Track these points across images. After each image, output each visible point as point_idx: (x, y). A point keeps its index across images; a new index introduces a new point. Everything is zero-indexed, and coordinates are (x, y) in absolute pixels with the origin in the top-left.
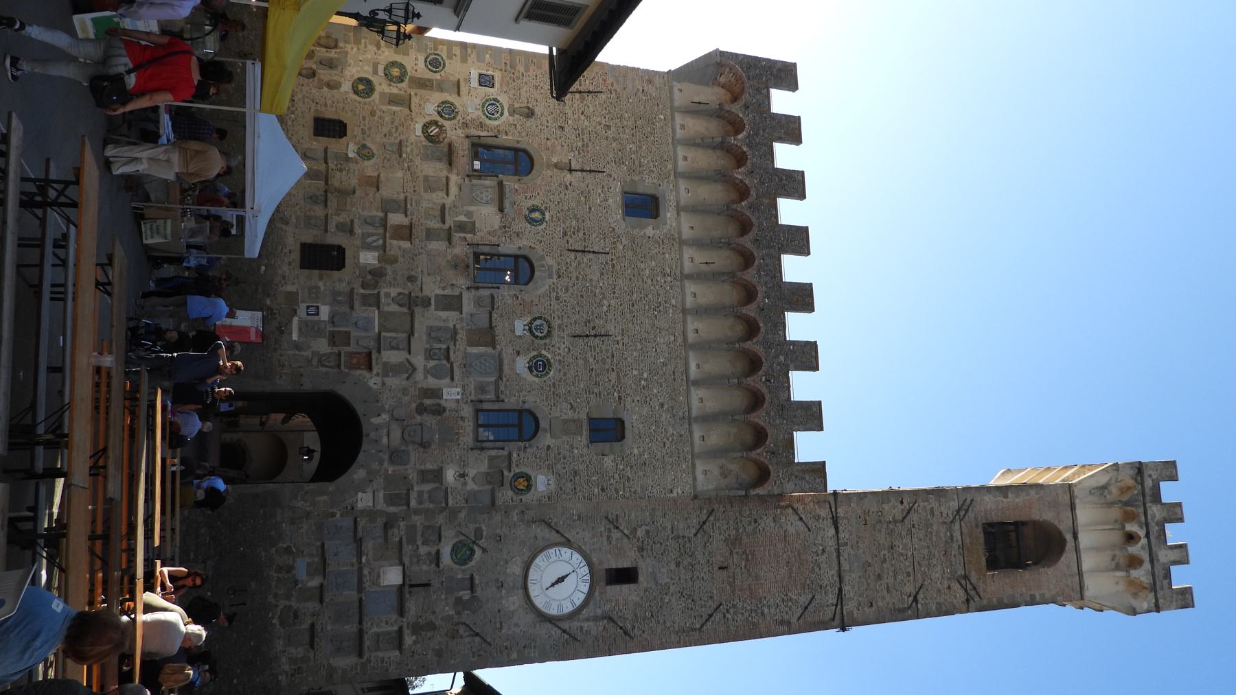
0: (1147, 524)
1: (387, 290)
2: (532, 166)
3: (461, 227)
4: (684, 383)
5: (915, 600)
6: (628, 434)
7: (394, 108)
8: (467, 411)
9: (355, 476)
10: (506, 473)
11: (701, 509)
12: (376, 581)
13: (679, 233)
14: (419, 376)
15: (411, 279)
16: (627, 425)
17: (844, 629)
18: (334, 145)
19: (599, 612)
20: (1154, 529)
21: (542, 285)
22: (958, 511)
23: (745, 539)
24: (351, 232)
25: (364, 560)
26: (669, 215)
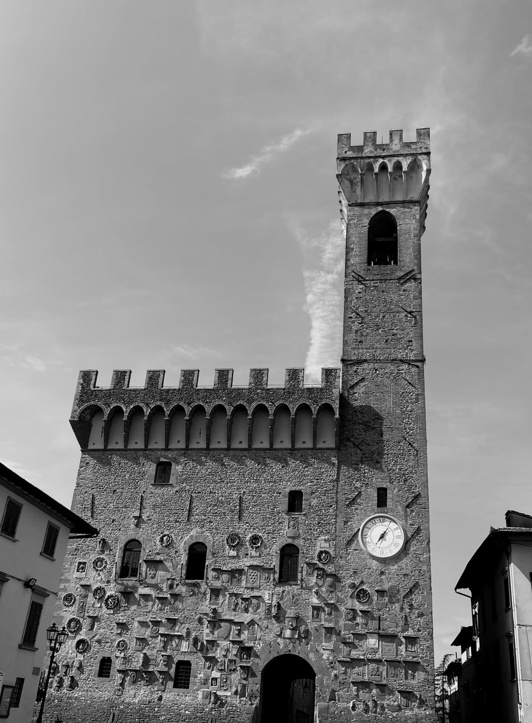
0: (376, 157)
3: (171, 587)
4: (271, 452)
5: (410, 313)
6: (297, 488)
7: (95, 626)
8: (279, 589)
9: (313, 660)
10: (317, 567)
11: (346, 446)
12: (375, 651)
13: (181, 449)
15: (200, 620)
16: (293, 489)
17: (425, 360)
18: (117, 664)
19: (402, 513)
20: (379, 152)
22: (360, 281)
23: (366, 419)
25: (362, 657)
26: (170, 455)
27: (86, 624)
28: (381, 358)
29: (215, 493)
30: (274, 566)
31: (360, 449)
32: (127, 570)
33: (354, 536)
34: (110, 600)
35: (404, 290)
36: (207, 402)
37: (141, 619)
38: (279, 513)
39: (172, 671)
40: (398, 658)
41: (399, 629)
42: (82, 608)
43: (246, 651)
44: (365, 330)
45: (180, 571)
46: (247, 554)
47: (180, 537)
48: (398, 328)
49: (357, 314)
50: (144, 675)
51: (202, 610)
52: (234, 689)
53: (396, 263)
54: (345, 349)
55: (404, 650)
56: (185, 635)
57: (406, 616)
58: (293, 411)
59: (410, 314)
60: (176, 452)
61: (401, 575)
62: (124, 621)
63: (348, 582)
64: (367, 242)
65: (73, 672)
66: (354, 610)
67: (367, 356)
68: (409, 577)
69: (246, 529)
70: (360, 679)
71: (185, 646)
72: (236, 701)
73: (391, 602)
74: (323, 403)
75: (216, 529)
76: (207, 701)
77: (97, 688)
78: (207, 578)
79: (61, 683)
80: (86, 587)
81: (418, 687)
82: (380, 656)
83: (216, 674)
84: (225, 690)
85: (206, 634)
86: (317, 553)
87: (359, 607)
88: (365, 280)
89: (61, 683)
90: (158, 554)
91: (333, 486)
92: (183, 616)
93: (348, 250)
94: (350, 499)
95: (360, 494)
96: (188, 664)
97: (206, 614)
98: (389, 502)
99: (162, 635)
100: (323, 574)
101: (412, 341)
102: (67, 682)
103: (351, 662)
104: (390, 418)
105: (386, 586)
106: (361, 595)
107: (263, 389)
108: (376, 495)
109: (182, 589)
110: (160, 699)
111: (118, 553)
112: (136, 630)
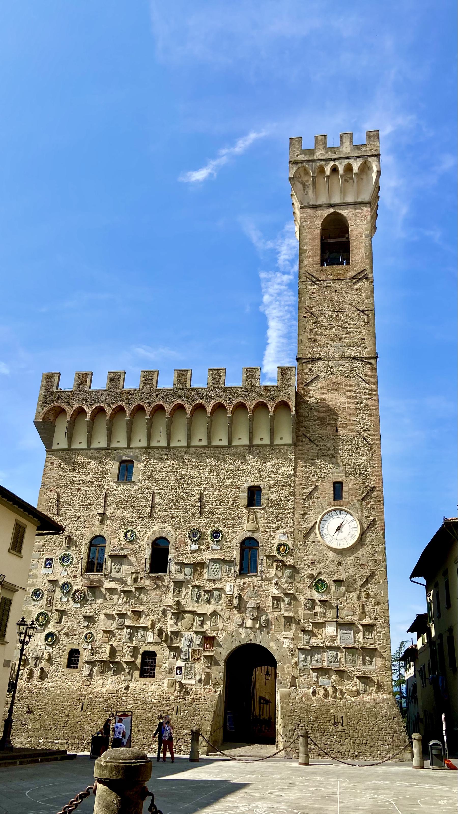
0: (327, 160)
1: (169, 626)
2: (102, 537)
3: (135, 580)
4: (230, 449)
5: (363, 311)
6: (256, 484)
7: (63, 620)
9: (274, 648)
10: (276, 559)
11: (302, 441)
12: (334, 639)
13: (143, 448)
14: (219, 608)
15: (164, 612)
16: (252, 484)
17: (378, 357)
18: (85, 656)
19: (358, 505)
20: (330, 155)
21: (171, 534)
22: (313, 282)
23: (321, 415)
24: (135, 648)
25: (321, 645)
26: (132, 454)
27: (54, 617)
28: (335, 356)
29: (176, 489)
30: (235, 559)
31: (316, 445)
32: (94, 565)
33: (311, 528)
34: (77, 594)
35: (357, 290)
36: (167, 402)
37: (108, 612)
38: (239, 507)
39: (138, 661)
40: (356, 645)
41: (357, 617)
42: (50, 602)
43: (209, 641)
44: (319, 329)
45: (144, 565)
46: (208, 548)
47: (143, 533)
48: (351, 326)
49: (312, 314)
50: (111, 665)
51: (166, 602)
52: (198, 678)
53: (348, 263)
54: (300, 348)
55: (362, 637)
56: (149, 627)
57: (363, 605)
58: (250, 410)
59: (363, 313)
60: (137, 451)
61: (358, 565)
62: (91, 614)
63: (306, 573)
64: (320, 243)
65: (43, 664)
66: (312, 600)
67: (322, 354)
68: (366, 567)
69: (207, 524)
70: (319, 665)
71: (150, 637)
72: (200, 688)
73: (349, 592)
74: (279, 400)
75: (178, 524)
76: (173, 689)
77: (66, 679)
78: (170, 572)
79: (31, 674)
80: (54, 582)
81: (376, 673)
82: (339, 643)
83: (180, 663)
84: (189, 678)
85: (170, 625)
86: (276, 545)
87: (317, 596)
88: (318, 280)
89: (31, 674)
90: (123, 549)
91: (291, 481)
92: (148, 608)
93: (302, 251)
94: (306, 493)
95: (316, 488)
96: (153, 654)
97: (170, 606)
98: (345, 496)
99: (128, 627)
100: (282, 566)
101: (365, 339)
102: (37, 674)
103: (311, 650)
104: (345, 414)
105: (343, 577)
106: (319, 584)
107: (221, 388)
108: (333, 489)
109: (146, 583)
110: (127, 688)
111: (84, 549)
112: (103, 623)
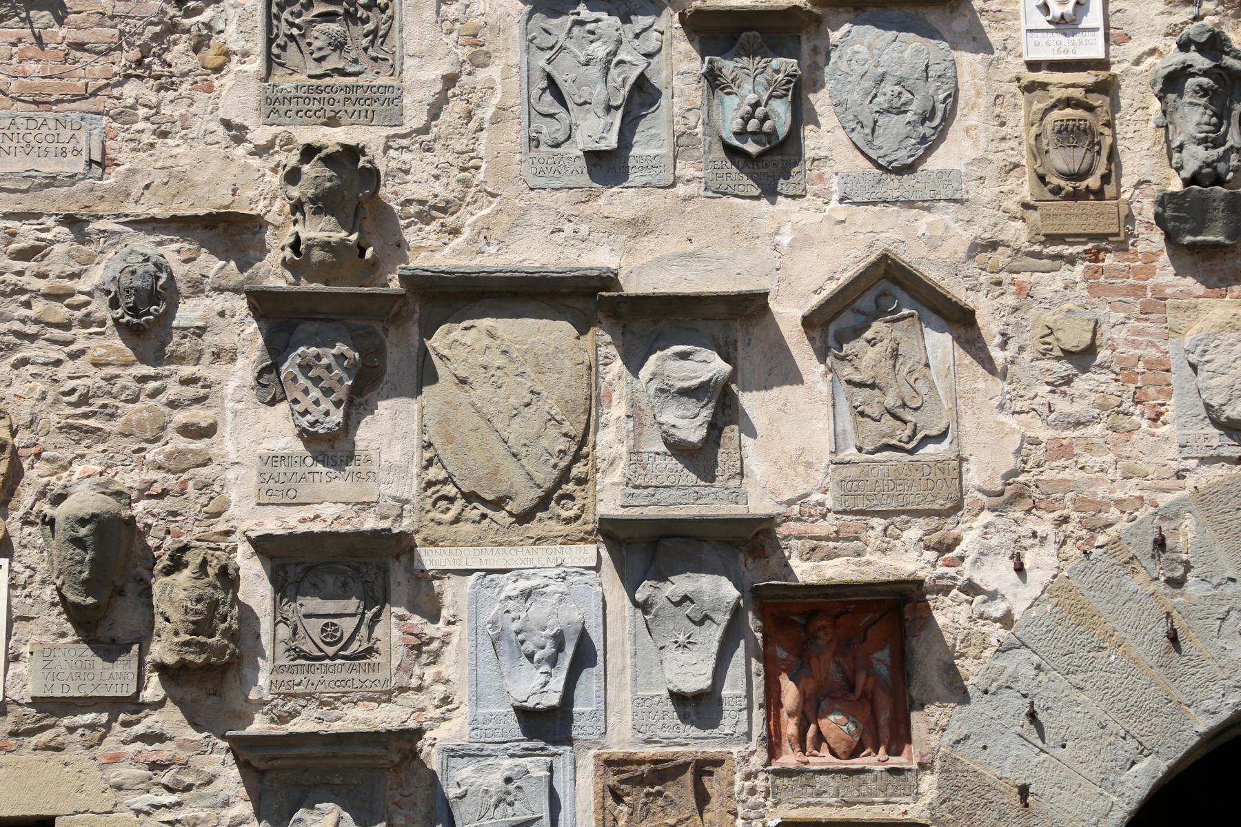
14: (932, 243)
